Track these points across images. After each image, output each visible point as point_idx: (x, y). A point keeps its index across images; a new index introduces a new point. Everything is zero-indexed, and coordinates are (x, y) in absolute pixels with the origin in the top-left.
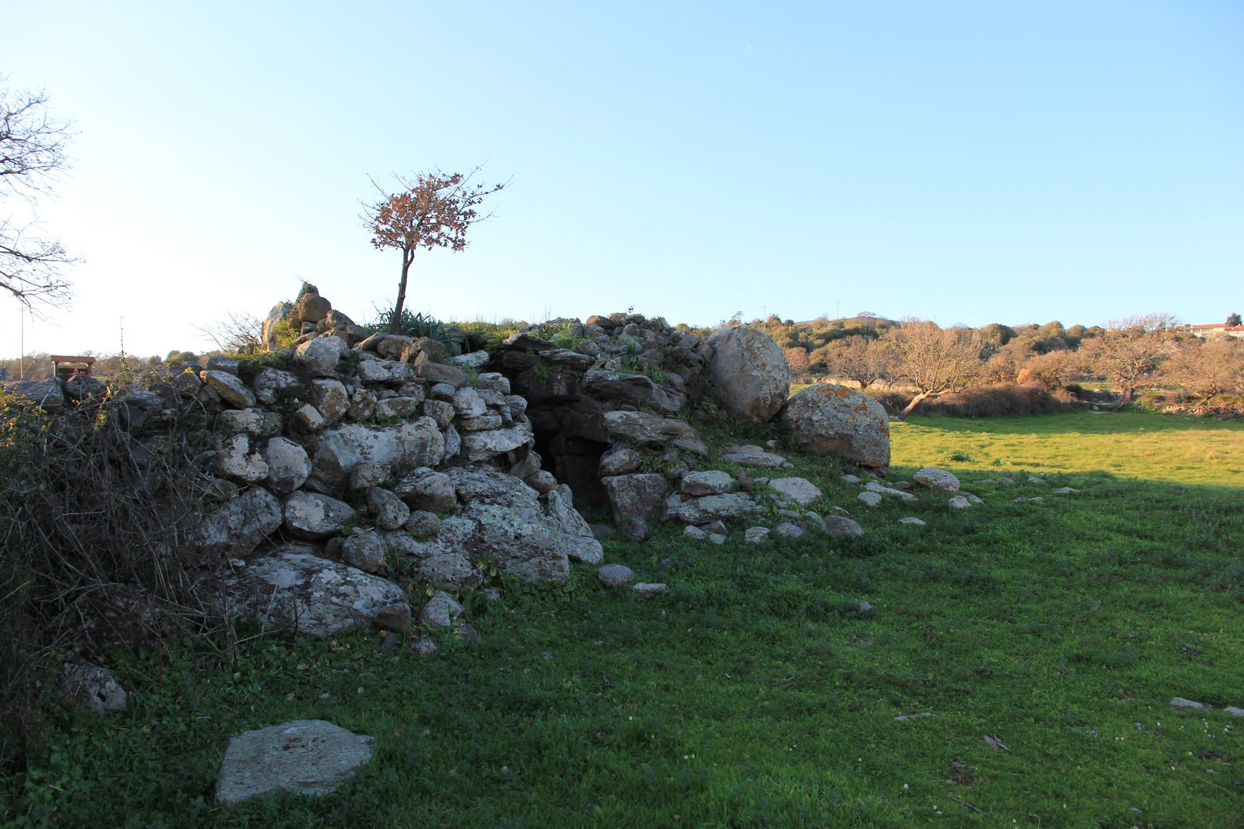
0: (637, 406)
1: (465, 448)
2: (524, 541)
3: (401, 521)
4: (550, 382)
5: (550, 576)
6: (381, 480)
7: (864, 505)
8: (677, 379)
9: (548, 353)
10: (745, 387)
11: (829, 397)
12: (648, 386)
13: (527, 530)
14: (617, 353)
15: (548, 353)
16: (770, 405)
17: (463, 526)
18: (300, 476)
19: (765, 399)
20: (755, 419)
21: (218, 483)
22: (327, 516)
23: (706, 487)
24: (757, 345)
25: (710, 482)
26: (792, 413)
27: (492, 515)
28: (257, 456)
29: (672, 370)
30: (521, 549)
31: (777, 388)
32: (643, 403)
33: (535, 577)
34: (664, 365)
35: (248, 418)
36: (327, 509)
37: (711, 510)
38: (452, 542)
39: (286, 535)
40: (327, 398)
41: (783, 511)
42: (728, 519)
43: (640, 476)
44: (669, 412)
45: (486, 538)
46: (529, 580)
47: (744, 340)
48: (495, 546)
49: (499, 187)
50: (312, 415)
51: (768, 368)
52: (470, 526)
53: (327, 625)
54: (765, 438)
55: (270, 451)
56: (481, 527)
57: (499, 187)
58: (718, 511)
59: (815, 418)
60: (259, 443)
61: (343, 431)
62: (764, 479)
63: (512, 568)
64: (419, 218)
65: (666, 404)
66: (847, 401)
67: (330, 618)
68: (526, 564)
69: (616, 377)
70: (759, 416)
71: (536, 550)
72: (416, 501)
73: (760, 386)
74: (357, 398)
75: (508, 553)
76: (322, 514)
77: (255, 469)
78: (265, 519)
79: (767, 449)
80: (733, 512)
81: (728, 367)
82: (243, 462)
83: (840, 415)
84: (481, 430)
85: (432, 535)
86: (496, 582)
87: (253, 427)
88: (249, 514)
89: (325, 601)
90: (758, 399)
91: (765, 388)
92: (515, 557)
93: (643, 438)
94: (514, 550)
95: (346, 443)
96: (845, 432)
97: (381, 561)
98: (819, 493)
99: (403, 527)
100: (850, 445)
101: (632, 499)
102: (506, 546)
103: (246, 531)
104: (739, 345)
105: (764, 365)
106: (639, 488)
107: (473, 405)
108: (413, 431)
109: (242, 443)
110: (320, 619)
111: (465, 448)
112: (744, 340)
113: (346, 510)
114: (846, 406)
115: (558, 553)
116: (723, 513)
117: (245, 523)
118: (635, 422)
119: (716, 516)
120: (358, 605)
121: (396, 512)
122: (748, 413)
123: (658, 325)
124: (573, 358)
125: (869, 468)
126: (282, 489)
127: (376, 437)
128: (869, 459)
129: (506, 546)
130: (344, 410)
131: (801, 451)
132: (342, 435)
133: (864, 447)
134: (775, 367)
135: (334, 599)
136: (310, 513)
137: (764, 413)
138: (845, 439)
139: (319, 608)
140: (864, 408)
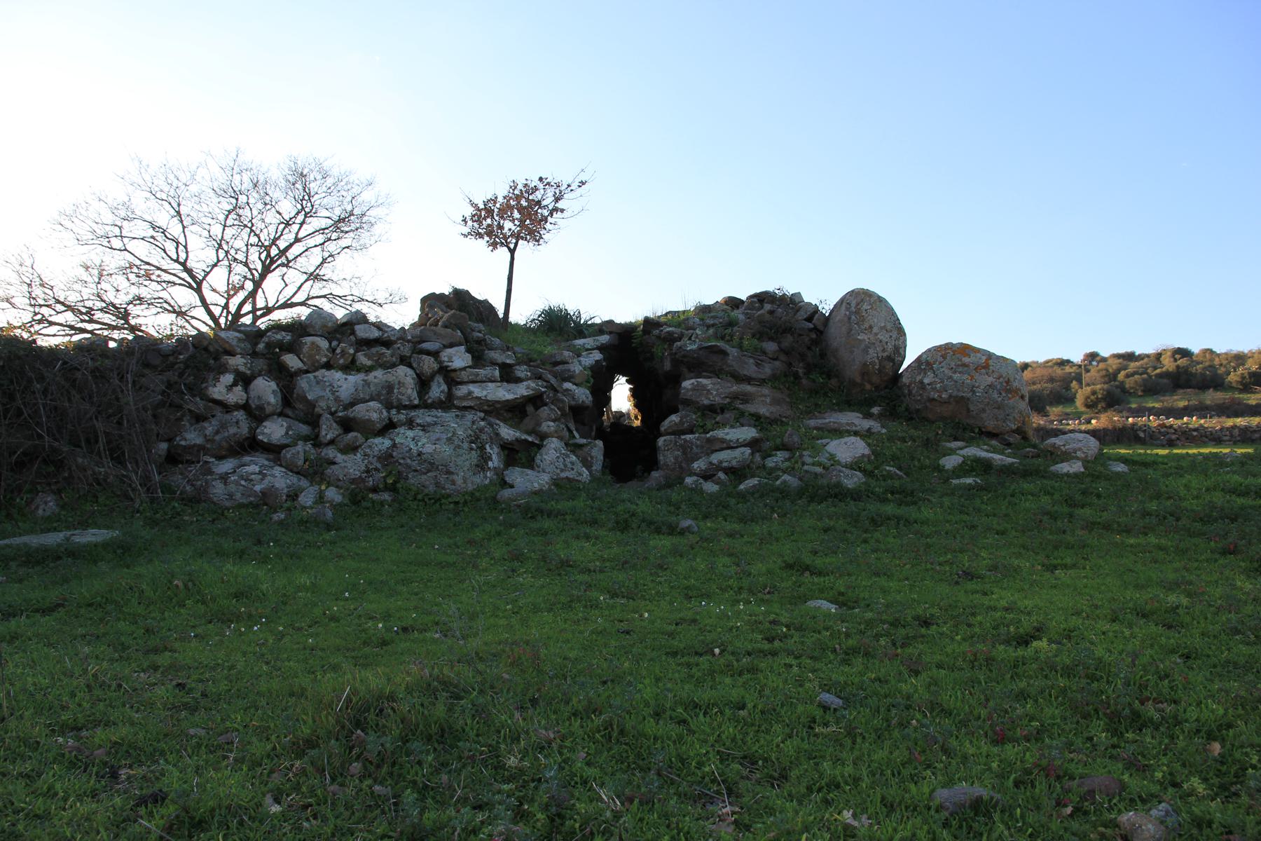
0: (717, 373)
1: (450, 396)
7: (940, 469)
8: (771, 347)
9: (656, 332)
10: (852, 352)
11: (944, 357)
12: (724, 353)
13: (429, 448)
14: (713, 325)
15: (656, 332)
16: (879, 370)
18: (269, 403)
19: (873, 363)
20: (868, 387)
21: (201, 404)
22: (287, 433)
23: (723, 441)
24: (865, 306)
25: (728, 437)
26: (905, 380)
27: (404, 436)
28: (239, 388)
29: (771, 339)
30: (420, 464)
31: (884, 350)
32: (721, 370)
33: (432, 488)
34: (760, 336)
35: (238, 362)
36: (289, 428)
37: (715, 461)
39: (251, 445)
40: (305, 349)
41: (806, 467)
42: (730, 471)
43: (688, 437)
44: (754, 379)
46: (426, 491)
47: (853, 305)
49: (583, 183)
50: (292, 361)
51: (875, 330)
54: (870, 402)
56: (394, 445)
57: (583, 183)
58: (721, 462)
59: (926, 381)
60: (245, 380)
62: (824, 441)
63: (414, 480)
64: (517, 218)
65: (750, 369)
66: (966, 360)
67: (238, 496)
68: (424, 477)
69: (694, 347)
70: (869, 382)
71: (432, 466)
72: (347, 425)
73: (866, 351)
74: (338, 351)
75: (409, 467)
76: (283, 431)
77: (237, 396)
78: (233, 430)
79: (868, 416)
80: (734, 463)
81: (836, 335)
82: (224, 391)
83: (956, 376)
85: (353, 449)
86: (392, 489)
87: (242, 369)
88: (223, 426)
89: (237, 483)
90: (865, 364)
91: (871, 351)
92: (416, 471)
93: (706, 402)
95: (318, 383)
96: (961, 394)
97: (300, 463)
98: (867, 451)
99: (332, 442)
100: (968, 410)
101: (676, 458)
104: (848, 309)
105: (871, 327)
106: (685, 448)
109: (228, 378)
110: (231, 496)
111: (450, 396)
112: (853, 305)
113: (304, 429)
114: (964, 365)
116: (725, 464)
117: (217, 432)
118: (704, 387)
119: (719, 468)
121: (329, 430)
122: (858, 380)
123: (791, 303)
125: (992, 435)
126: (257, 415)
128: (990, 425)
130: (325, 359)
131: (912, 417)
133: (984, 410)
134: (882, 328)
135: (243, 482)
136: (274, 431)
137: (875, 379)
138: (961, 401)
139: (232, 488)
140: (986, 367)
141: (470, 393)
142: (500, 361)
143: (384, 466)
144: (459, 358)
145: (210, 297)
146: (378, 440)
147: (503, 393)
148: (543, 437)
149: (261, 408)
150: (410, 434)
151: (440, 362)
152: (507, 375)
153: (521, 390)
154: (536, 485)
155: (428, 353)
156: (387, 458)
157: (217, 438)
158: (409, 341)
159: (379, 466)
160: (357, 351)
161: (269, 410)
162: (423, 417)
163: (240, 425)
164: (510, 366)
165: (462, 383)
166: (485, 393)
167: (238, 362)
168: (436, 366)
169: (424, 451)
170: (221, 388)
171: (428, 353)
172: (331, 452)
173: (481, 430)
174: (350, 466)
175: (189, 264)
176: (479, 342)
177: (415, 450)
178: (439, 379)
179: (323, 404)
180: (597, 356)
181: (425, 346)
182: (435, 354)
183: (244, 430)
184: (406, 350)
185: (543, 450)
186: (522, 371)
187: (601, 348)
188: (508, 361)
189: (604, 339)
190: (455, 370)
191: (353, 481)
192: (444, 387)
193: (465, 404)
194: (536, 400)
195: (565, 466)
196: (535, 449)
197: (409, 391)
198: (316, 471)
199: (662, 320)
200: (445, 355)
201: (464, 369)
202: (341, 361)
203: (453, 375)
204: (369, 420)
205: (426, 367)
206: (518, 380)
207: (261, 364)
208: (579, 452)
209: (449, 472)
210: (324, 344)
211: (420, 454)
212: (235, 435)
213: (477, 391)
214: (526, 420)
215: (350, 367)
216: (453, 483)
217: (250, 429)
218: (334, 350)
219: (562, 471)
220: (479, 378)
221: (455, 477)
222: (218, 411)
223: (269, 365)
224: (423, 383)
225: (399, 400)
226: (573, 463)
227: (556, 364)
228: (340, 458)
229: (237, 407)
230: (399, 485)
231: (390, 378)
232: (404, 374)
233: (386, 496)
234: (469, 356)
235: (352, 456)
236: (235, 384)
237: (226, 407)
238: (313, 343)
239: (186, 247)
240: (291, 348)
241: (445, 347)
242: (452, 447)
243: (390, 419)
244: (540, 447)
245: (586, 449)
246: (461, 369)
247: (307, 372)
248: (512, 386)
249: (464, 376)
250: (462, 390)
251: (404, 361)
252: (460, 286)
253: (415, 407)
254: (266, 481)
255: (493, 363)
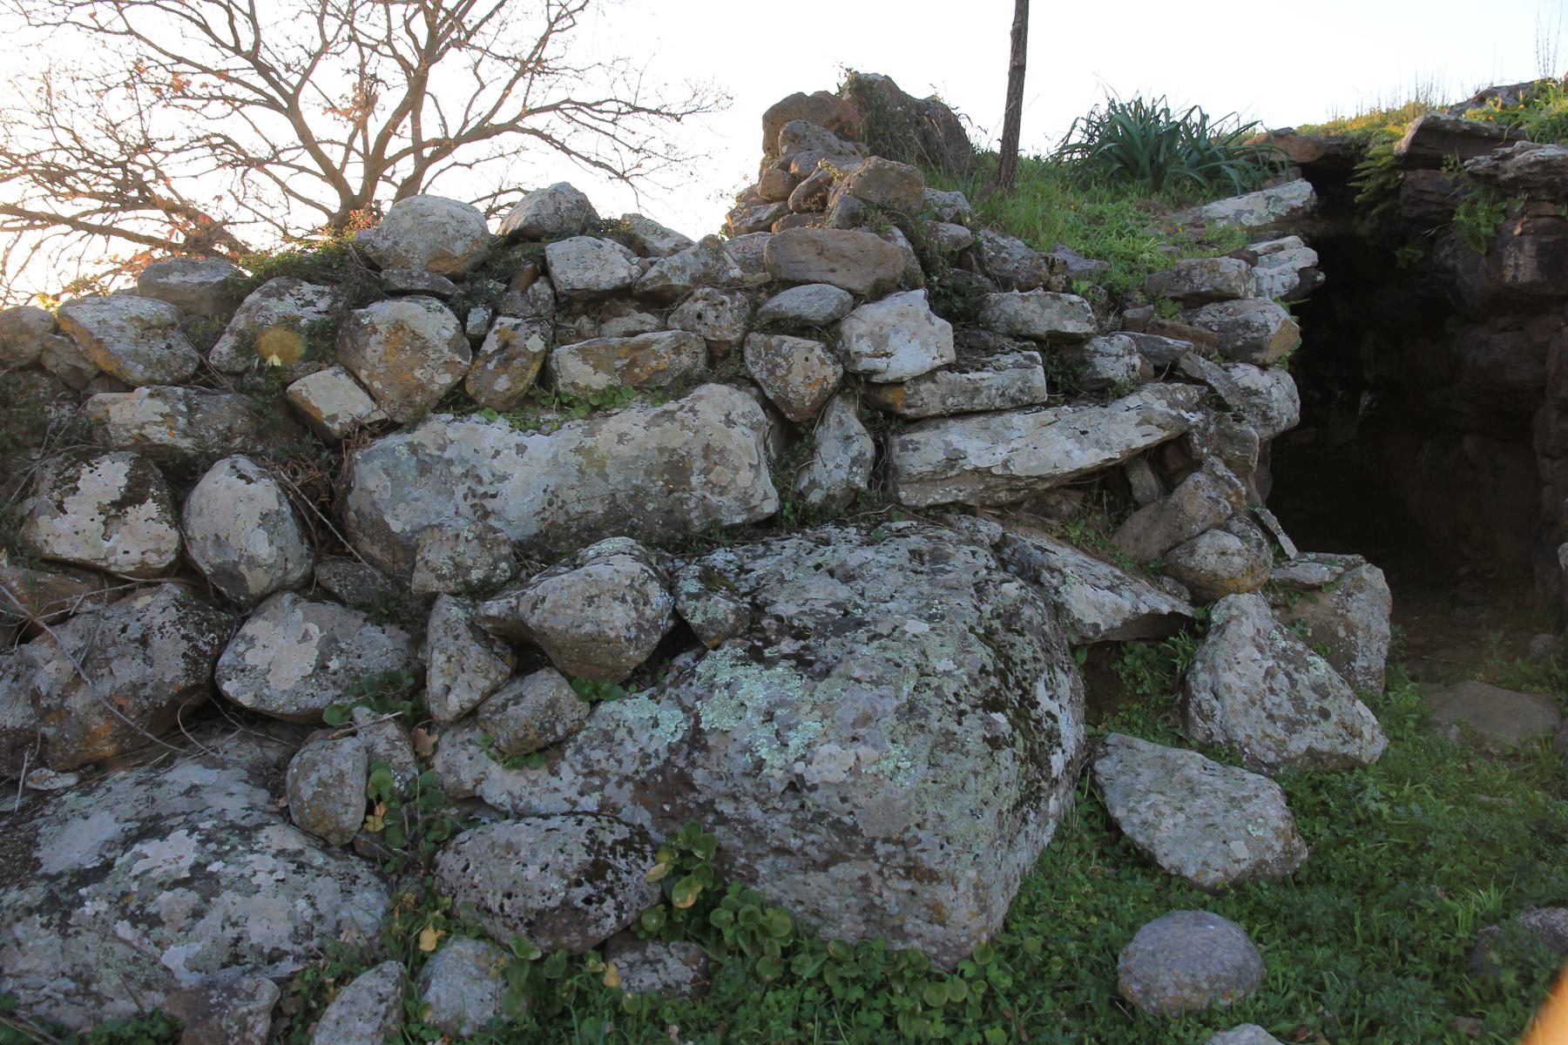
1: (882, 469)
2: (814, 799)
3: (454, 703)
4: (1495, 247)
5: (905, 937)
6: (476, 575)
9: (1482, 162)
13: (830, 764)
15: (1482, 162)
17: (646, 723)
18: (252, 562)
27: (740, 698)
28: (150, 508)
30: (800, 826)
33: (849, 927)
36: (330, 645)
38: (603, 775)
39: (203, 712)
40: (374, 349)
45: (699, 776)
48: (727, 808)
50: (332, 396)
52: (672, 724)
53: (100, 999)
55: (196, 498)
56: (696, 739)
60: (172, 476)
61: (417, 436)
67: (109, 982)
68: (817, 879)
71: (848, 839)
72: (524, 650)
74: (491, 345)
75: (758, 836)
76: (306, 659)
77: (144, 537)
78: (127, 671)
84: (961, 415)
85: (542, 750)
86: (697, 926)
87: (160, 435)
92: (782, 851)
94: (779, 824)
95: (424, 469)
97: (351, 817)
102: (755, 812)
103: (77, 701)
107: (894, 342)
108: (639, 433)
110: (84, 980)
111: (882, 469)
115: (931, 860)
120: (175, 957)
121: (458, 673)
124: (1546, 165)
127: (521, 449)
129: (755, 812)
130: (446, 379)
132: (413, 449)
135: (124, 929)
139: (87, 948)
141: (954, 459)
142: (1041, 328)
143: (661, 818)
144: (907, 339)
145: (323, 126)
146: (634, 709)
147: (1062, 445)
148: (1205, 592)
149: (230, 575)
150: (757, 685)
151: (845, 358)
152: (1072, 379)
153: (1122, 430)
154: (1240, 849)
155: (802, 328)
156: (667, 785)
157: (77, 701)
158: (733, 287)
159: (643, 817)
160: (554, 341)
161: (257, 581)
162: (800, 581)
163: (155, 646)
164: (1077, 341)
165: (919, 422)
166: (1002, 452)
167: (138, 413)
168: (831, 373)
169: (812, 774)
170: (85, 517)
171: (802, 328)
172: (463, 762)
173: (1009, 618)
174: (528, 850)
175: (265, 56)
176: (963, 256)
177: (776, 768)
178: (846, 417)
179: (436, 555)
180: (1298, 256)
181: (790, 302)
182: (827, 331)
183: (170, 666)
184: (726, 323)
185: (1216, 649)
186: (1116, 357)
187: (1287, 223)
188: (1071, 327)
189: (1299, 192)
190: (898, 383)
191: (535, 923)
192: (865, 445)
193: (937, 496)
194: (1170, 458)
195: (1299, 704)
196: (1182, 640)
197: (745, 478)
198: (409, 841)
199: (1472, 116)
200: (860, 331)
201: (931, 375)
202: (502, 384)
203: (890, 396)
204: (596, 639)
205: (796, 379)
206: (1105, 392)
207: (224, 411)
208: (1305, 610)
209: (913, 871)
210: (436, 324)
211: (796, 786)
212: (135, 688)
213: (976, 446)
214: (1137, 523)
215: (540, 397)
216: (937, 915)
217: (193, 659)
218: (477, 342)
219: (1292, 726)
220: (980, 402)
221: (943, 892)
222: (80, 596)
223: (256, 414)
224: (791, 434)
225: (707, 510)
226: (1321, 690)
227: (1196, 301)
228: (500, 784)
229: (149, 578)
230: (721, 916)
231: (675, 437)
232: (724, 419)
233: (676, 966)
234: (943, 330)
235: (541, 774)
236: (133, 496)
237: (116, 585)
238: (398, 326)
239: (252, 17)
240: (329, 343)
241: (858, 299)
242: (922, 744)
243: (676, 614)
244: (1198, 629)
245: (1328, 600)
246: (917, 379)
247: (388, 427)
248: (1090, 415)
249: (930, 398)
250: (923, 452)
251: (722, 362)
252: (868, 66)
253: (766, 528)
254: (213, 919)
255: (1022, 337)
